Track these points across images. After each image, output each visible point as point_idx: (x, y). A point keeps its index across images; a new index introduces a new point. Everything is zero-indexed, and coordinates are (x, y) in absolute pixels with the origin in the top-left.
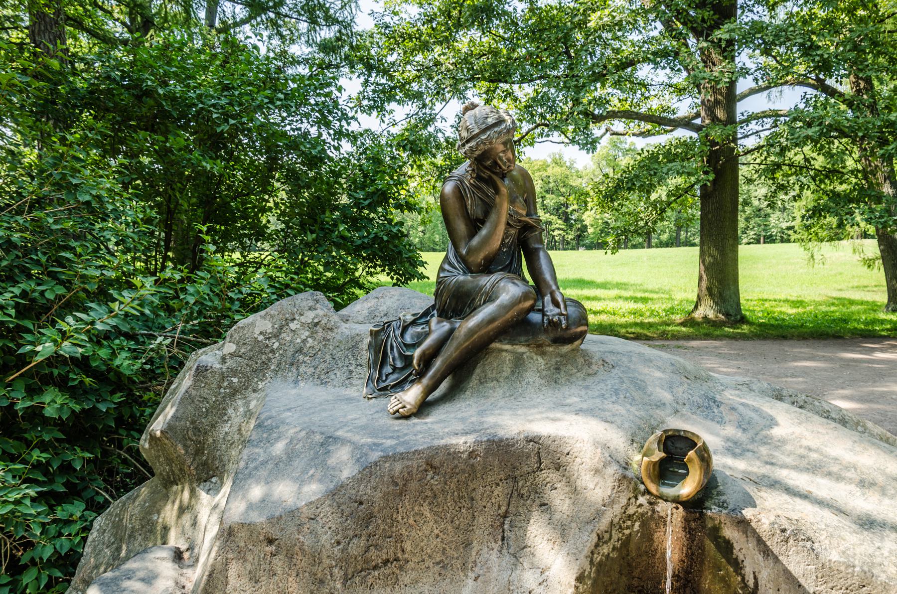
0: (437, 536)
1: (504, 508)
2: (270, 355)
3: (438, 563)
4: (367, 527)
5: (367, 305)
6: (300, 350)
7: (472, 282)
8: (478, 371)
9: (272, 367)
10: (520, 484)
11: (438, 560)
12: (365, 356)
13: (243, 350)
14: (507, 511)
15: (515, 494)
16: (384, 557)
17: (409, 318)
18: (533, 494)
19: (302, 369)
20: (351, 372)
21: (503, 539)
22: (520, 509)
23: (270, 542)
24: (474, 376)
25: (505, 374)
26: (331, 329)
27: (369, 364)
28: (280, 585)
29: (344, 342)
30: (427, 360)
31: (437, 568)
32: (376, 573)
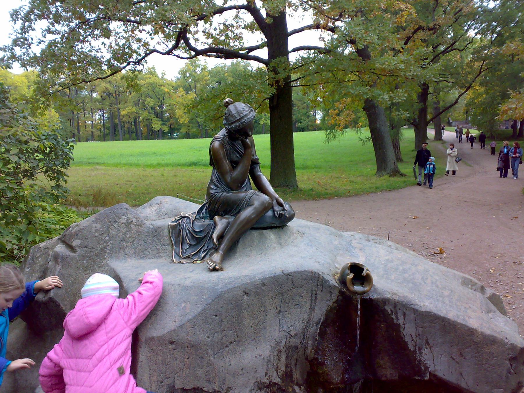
0: (252, 327)
1: (279, 309)
4: (221, 327)
6: (124, 240)
9: (108, 251)
10: (285, 296)
16: (230, 341)
18: (291, 300)
22: (286, 309)
23: (172, 343)
26: (140, 225)
28: (180, 364)
29: (150, 232)
31: (253, 342)
32: (227, 349)
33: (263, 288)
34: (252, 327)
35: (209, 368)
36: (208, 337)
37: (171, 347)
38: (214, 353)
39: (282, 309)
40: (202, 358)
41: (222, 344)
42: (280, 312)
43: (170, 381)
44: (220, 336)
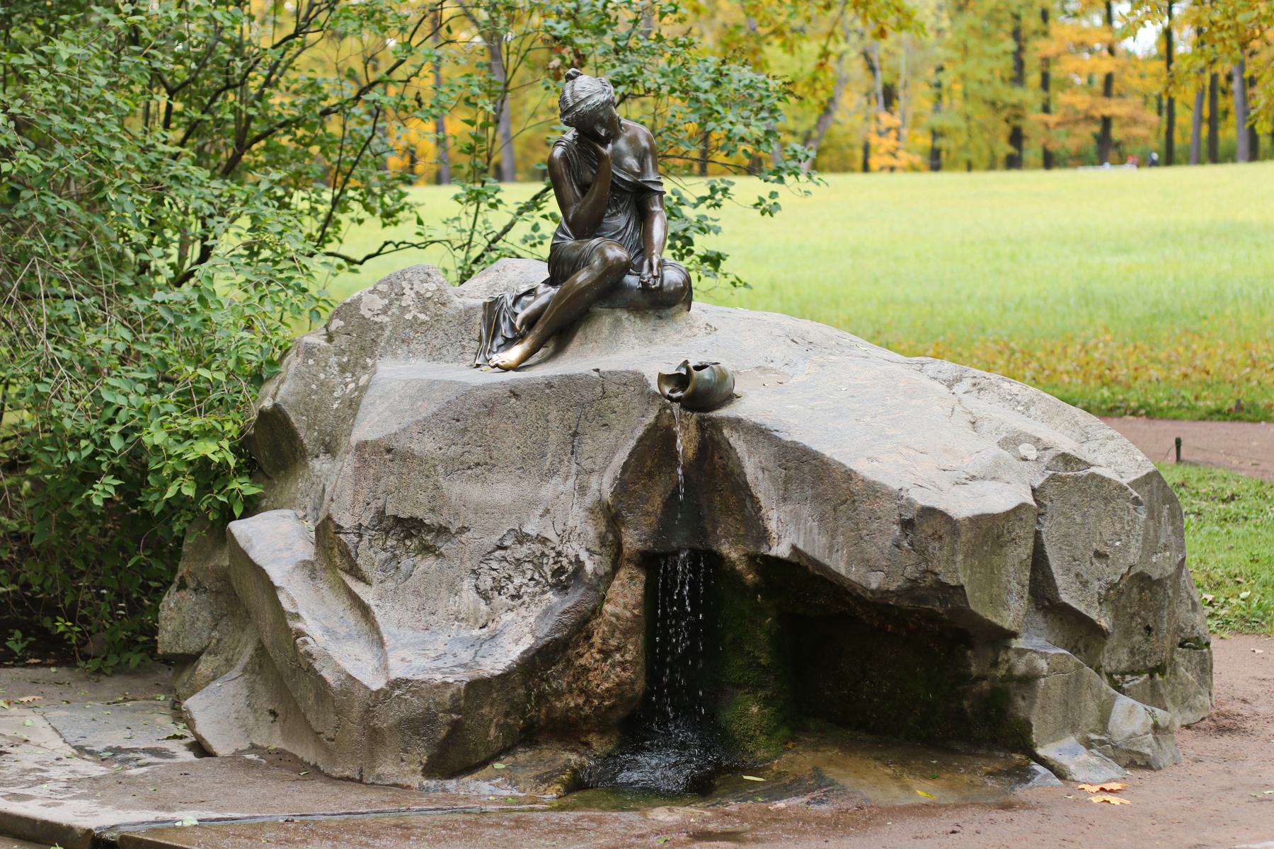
0: (519, 448)
2: (379, 332)
3: (519, 469)
5: (485, 280)
7: (575, 248)
8: (580, 334)
11: (519, 466)
12: (478, 326)
13: (350, 328)
14: (575, 432)
15: (583, 417)
16: (476, 461)
17: (523, 290)
19: (413, 346)
20: (464, 347)
21: (572, 453)
22: (587, 430)
23: (389, 451)
24: (575, 339)
25: (603, 336)
26: (444, 304)
27: (480, 337)
30: (531, 321)
32: (469, 472)
33: (547, 391)
34: (519, 448)
35: (434, 493)
36: (440, 449)
37: (390, 456)
38: (446, 472)
39: (580, 430)
40: (427, 477)
41: (462, 463)
42: (575, 434)
43: (380, 503)
44: (459, 449)
